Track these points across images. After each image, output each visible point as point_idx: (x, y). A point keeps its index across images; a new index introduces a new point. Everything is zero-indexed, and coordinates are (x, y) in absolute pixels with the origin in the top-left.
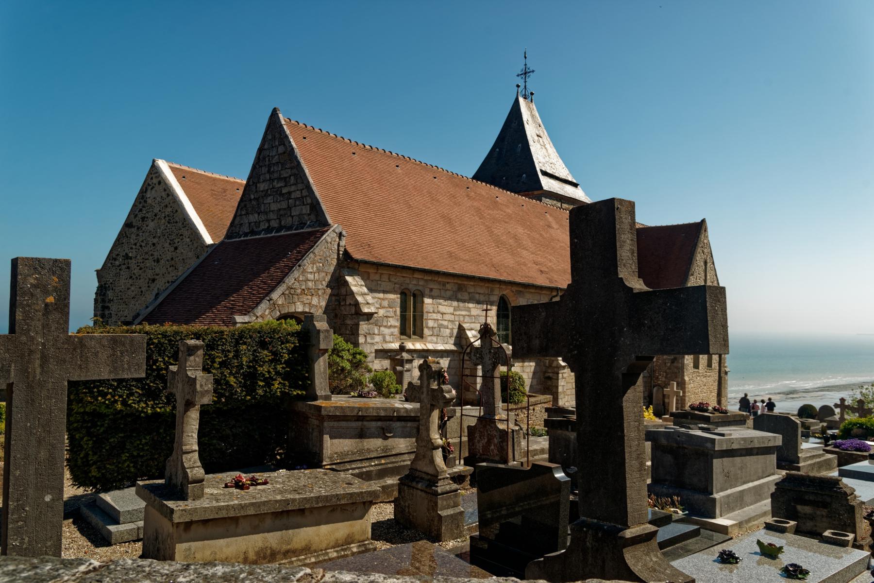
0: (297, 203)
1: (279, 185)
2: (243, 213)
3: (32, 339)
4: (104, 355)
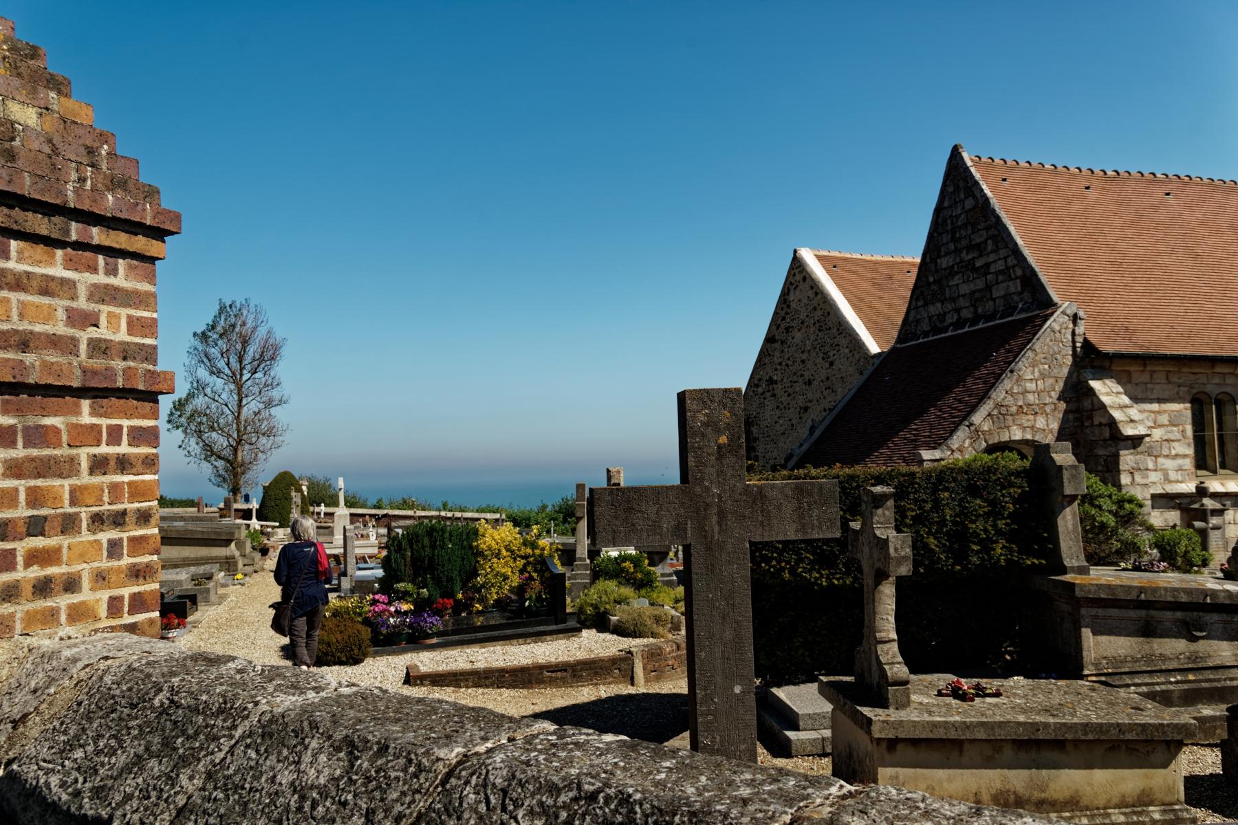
0: (1000, 278)
1: (970, 257)
2: (920, 304)
3: (707, 489)
4: (788, 508)
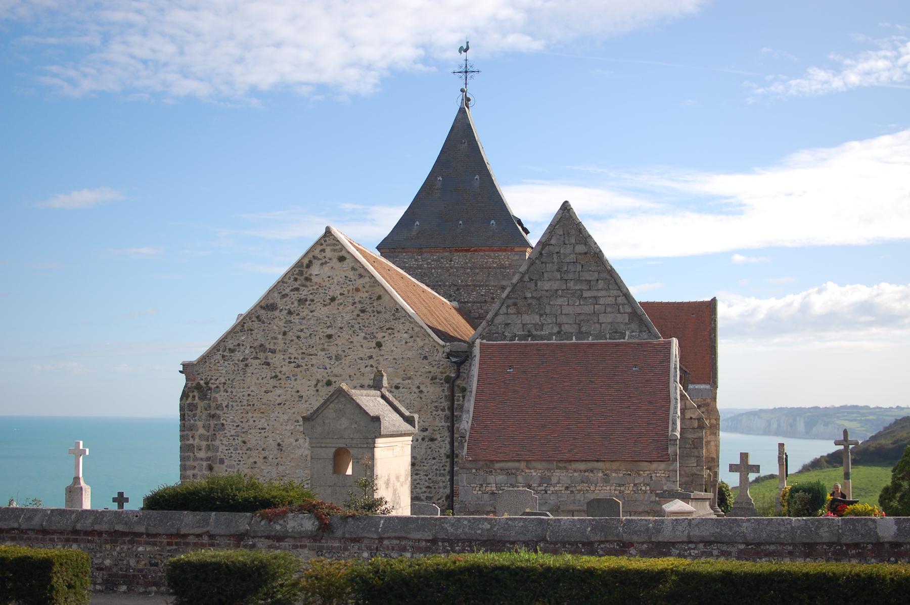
0: (609, 310)
1: (577, 288)
